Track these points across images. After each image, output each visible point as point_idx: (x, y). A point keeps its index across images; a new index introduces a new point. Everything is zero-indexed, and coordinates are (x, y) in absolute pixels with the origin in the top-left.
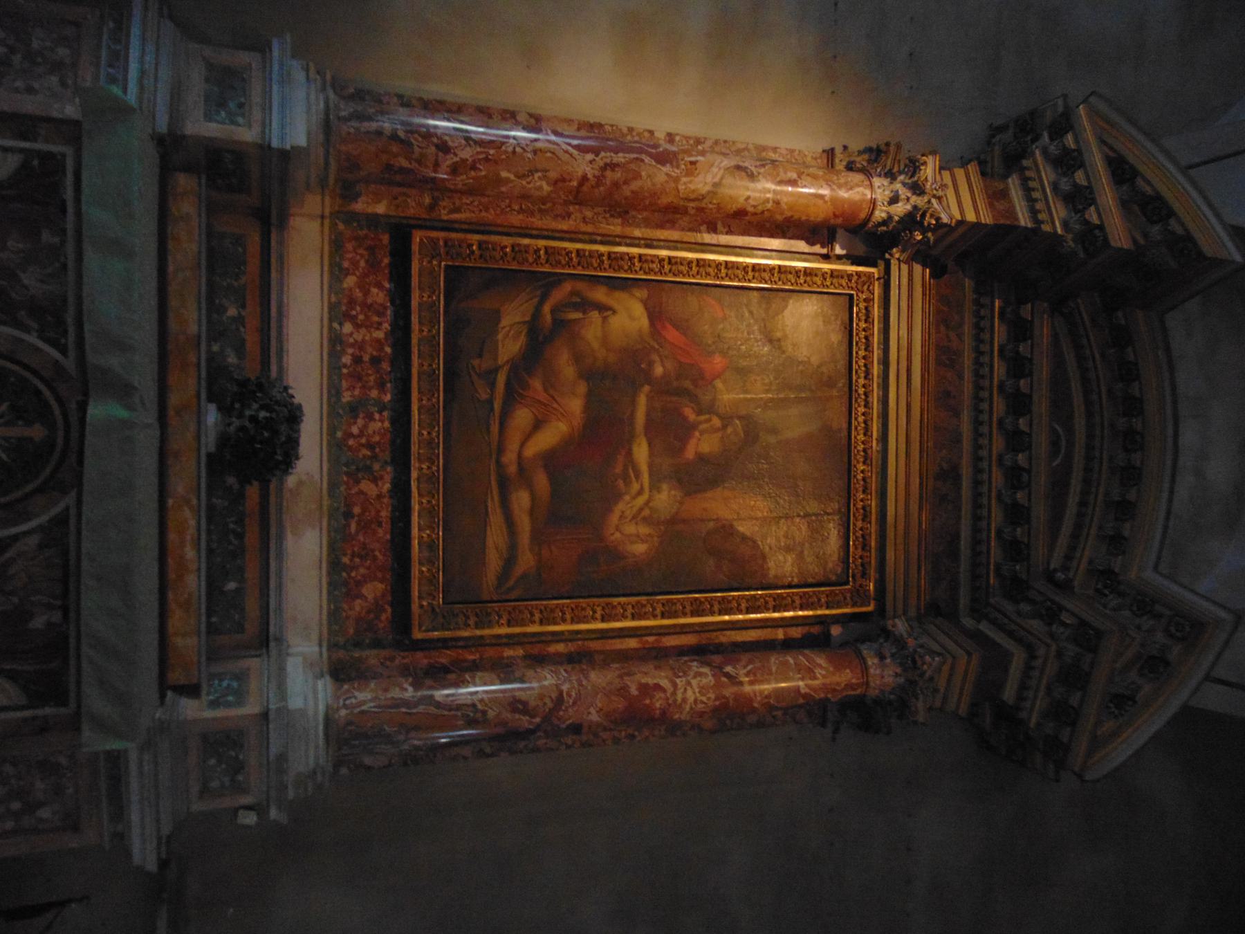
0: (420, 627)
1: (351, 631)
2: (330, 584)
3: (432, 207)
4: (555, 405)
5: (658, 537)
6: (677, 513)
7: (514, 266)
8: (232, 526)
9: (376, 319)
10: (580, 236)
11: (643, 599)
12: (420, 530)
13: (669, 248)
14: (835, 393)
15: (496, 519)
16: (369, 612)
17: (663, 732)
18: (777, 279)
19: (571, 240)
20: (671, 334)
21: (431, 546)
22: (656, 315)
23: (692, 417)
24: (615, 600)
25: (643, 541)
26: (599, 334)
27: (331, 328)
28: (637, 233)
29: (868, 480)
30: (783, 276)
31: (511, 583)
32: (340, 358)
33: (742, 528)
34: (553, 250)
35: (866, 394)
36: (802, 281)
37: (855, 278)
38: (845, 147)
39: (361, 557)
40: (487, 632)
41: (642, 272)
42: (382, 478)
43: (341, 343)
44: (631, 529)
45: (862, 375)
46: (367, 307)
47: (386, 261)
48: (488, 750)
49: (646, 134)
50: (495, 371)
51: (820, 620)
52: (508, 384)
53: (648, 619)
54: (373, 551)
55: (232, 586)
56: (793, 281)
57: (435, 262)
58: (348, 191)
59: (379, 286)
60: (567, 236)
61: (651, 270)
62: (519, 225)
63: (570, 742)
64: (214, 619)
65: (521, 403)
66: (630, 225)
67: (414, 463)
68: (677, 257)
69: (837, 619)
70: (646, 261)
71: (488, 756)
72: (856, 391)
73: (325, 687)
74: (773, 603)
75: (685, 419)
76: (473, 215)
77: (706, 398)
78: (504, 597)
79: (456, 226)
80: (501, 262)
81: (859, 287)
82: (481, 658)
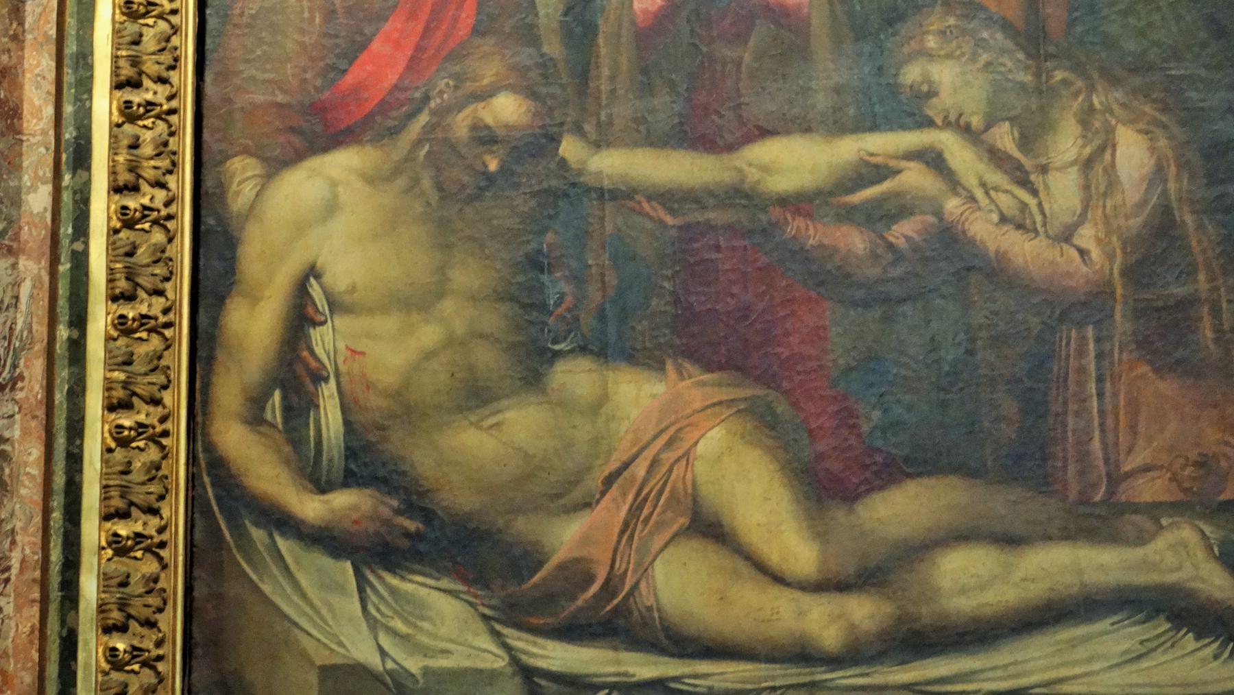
4: (640, 469)
5: (1091, 89)
6: (1006, 26)
7: (173, 621)
10: (59, 397)
13: (85, 85)
19: (76, 429)
25: (1108, 144)
26: (388, 324)
28: (38, 200)
34: (114, 493)
41: (171, 181)
50: (527, 673)
52: (570, 632)
60: (61, 442)
61: (162, 147)
62: (36, 610)
65: (637, 584)
68: (115, 58)
70: (133, 168)
80: (161, 667)
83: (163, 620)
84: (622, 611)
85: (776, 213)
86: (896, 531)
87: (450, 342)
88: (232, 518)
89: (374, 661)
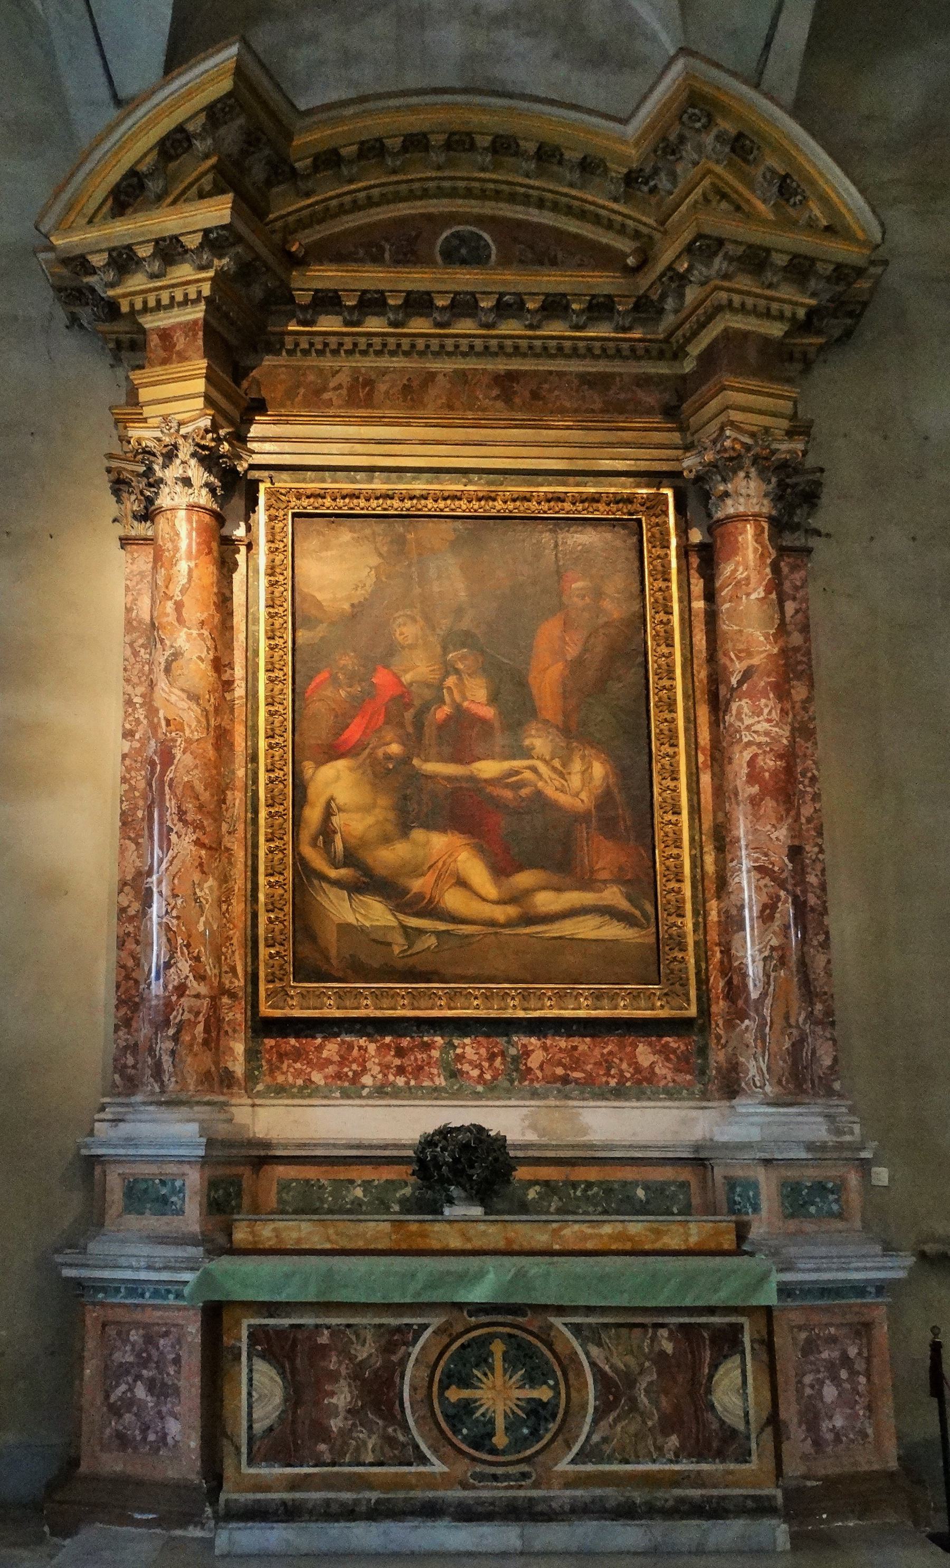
0: (681, 1008)
1: (688, 1077)
2: (638, 1099)
3: (233, 995)
4: (440, 864)
6: (557, 727)
7: (289, 908)
8: (579, 1193)
9: (355, 1052)
11: (656, 767)
12: (580, 1009)
13: (255, 735)
14: (411, 537)
15: (566, 928)
16: (668, 1059)
17: (809, 744)
18: (281, 609)
19: (255, 846)
20: (354, 733)
21: (598, 996)
22: (332, 752)
23: (447, 709)
24: (657, 798)
25: (590, 766)
26: (358, 816)
27: (369, 1097)
28: (241, 773)
29: (515, 496)
30: (278, 602)
31: (637, 913)
32: (399, 1088)
33: (572, 652)
35: (411, 498)
36: (281, 578)
37: (273, 512)
38: (115, 520)
39: (608, 1069)
40: (690, 940)
42: (524, 1046)
43: (383, 1086)
44: (576, 781)
45: (389, 502)
46: (344, 1060)
47: (293, 1041)
48: (821, 938)
49: (128, 762)
50: (404, 928)
51: (685, 551)
52: (419, 914)
53: (678, 763)
54: (602, 1055)
55: (640, 1193)
56: (282, 589)
57: (292, 993)
58: (227, 1080)
59: (320, 1048)
60: (250, 850)
63: (816, 849)
64: (675, 1211)
66: (232, 780)
67: (509, 1014)
69: (683, 532)
71: (827, 938)
72: (408, 510)
73: (744, 1105)
74: (662, 614)
75: (449, 717)
76: (237, 953)
77: (428, 694)
78: (653, 920)
79: (249, 969)
81: (283, 506)
82: (719, 944)
83: (286, 908)
84: (435, 908)
85: (483, 784)
86: (521, 887)
87: (377, 822)
88: (307, 877)
89: (355, 922)
